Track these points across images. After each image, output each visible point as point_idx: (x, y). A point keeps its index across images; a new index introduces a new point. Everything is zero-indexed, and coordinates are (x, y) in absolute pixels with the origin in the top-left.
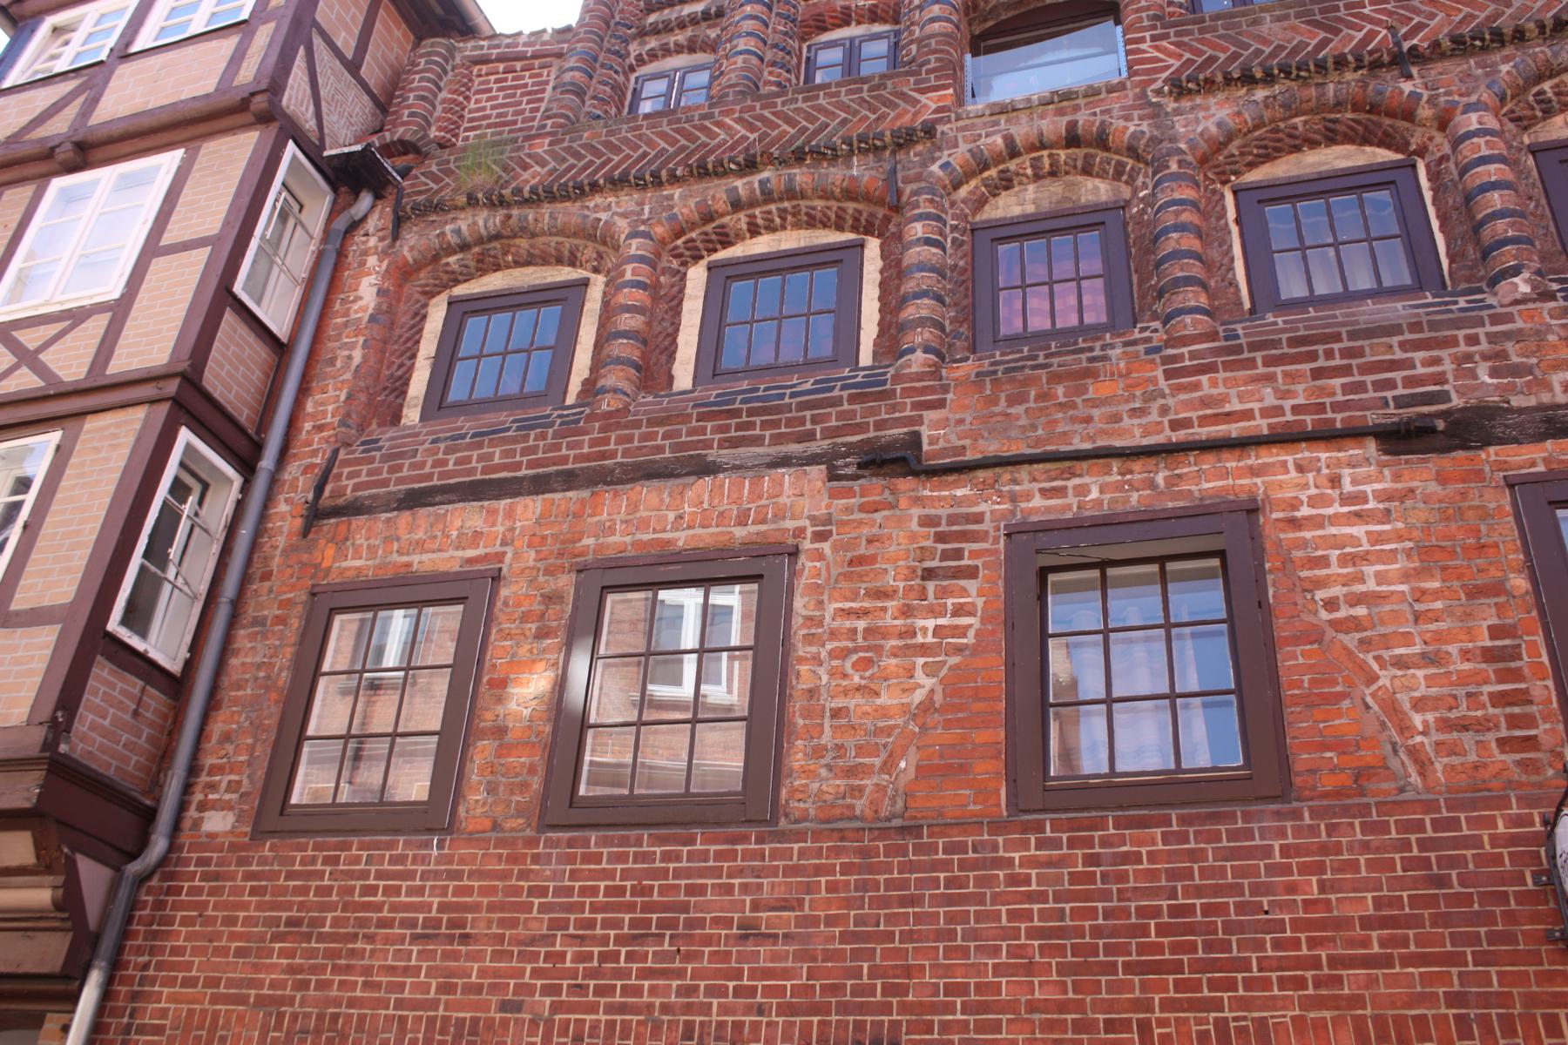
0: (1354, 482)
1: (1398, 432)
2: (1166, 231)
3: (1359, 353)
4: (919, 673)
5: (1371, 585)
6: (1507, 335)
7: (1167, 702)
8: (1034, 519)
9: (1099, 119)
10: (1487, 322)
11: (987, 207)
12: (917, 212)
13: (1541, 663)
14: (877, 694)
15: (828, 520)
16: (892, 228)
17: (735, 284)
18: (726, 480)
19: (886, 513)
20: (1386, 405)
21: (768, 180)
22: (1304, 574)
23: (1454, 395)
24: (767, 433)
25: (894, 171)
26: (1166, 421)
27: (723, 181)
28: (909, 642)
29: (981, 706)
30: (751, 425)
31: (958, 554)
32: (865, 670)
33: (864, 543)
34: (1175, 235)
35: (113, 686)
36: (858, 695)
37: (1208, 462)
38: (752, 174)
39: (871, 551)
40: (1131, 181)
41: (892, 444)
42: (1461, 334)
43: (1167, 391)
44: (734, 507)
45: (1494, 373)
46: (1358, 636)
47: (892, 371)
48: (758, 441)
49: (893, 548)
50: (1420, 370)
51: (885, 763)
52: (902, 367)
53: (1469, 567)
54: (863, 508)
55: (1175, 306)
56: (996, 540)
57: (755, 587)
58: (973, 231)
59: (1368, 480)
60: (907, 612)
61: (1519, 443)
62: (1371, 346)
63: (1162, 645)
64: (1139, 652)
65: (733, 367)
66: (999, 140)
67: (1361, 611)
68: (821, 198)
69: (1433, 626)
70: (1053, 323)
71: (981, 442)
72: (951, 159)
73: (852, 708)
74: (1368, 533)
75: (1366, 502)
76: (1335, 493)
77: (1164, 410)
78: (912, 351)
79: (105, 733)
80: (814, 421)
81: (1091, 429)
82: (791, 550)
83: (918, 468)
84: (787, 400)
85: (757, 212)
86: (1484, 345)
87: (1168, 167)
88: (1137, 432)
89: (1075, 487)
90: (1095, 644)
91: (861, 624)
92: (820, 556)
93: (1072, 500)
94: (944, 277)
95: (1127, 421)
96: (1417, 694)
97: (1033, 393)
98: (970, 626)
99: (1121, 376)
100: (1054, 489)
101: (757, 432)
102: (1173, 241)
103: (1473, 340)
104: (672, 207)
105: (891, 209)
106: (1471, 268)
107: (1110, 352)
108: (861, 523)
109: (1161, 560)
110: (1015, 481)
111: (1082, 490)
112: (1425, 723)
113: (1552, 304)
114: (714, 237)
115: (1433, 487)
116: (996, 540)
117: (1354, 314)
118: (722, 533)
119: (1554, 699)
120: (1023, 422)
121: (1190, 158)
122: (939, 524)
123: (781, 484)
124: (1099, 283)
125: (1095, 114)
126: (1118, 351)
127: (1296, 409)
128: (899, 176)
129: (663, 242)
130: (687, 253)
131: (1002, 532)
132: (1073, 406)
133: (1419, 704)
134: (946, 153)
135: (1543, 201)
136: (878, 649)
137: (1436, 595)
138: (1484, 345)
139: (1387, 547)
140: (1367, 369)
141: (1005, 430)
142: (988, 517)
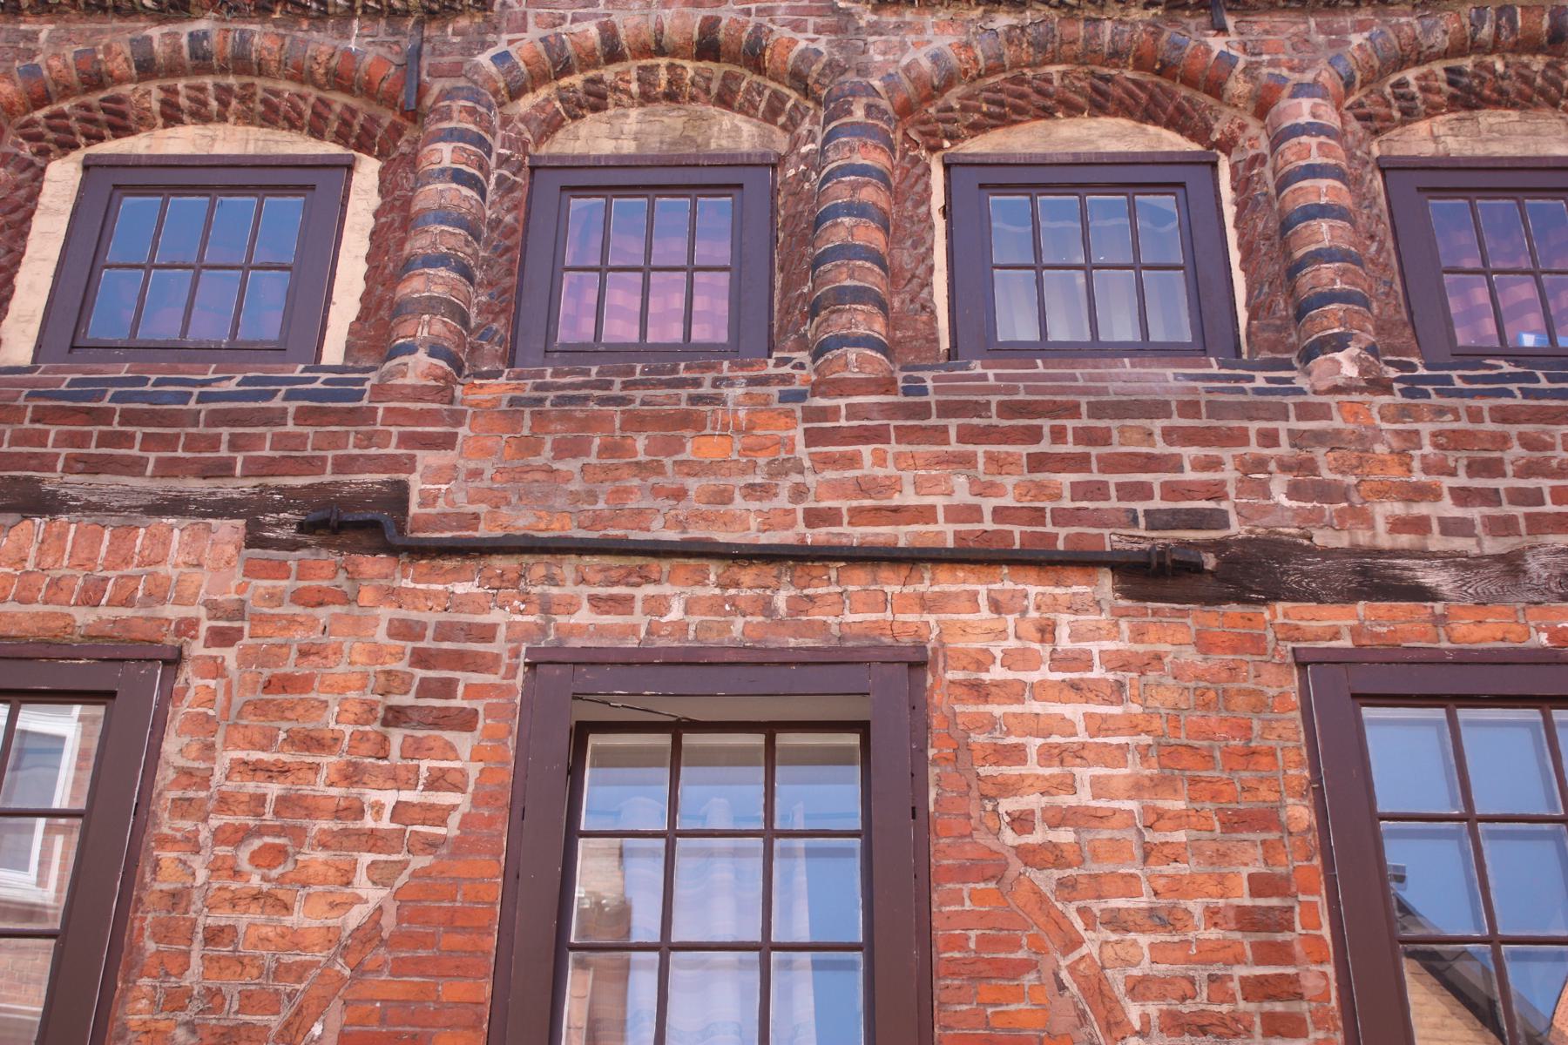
0: (1075, 636)
1: (1147, 565)
2: (835, 212)
3: (1103, 438)
4: (361, 878)
5: (1084, 798)
6: (1319, 438)
7: (755, 955)
8: (576, 643)
9: (753, 20)
10: (1292, 414)
11: (560, 134)
12: (446, 125)
13: (1320, 938)
14: (287, 908)
15: (239, 612)
16: (403, 146)
17: (128, 200)
18: (70, 527)
19: (337, 609)
20: (1135, 521)
21: (205, 35)
22: (986, 770)
23: (1233, 519)
24: (152, 456)
25: (417, 53)
26: (799, 510)
27: (128, 24)
28: (351, 825)
29: (458, 939)
30: (127, 440)
31: (447, 689)
32: (270, 867)
33: (294, 654)
34: (846, 220)
36: (254, 907)
37: (857, 581)
38: (180, 20)
39: (305, 669)
40: (791, 126)
41: (360, 498)
42: (1254, 427)
43: (807, 463)
44: (80, 573)
45: (1294, 491)
46: (1057, 874)
47: (373, 378)
48: (134, 467)
49: (342, 668)
50: (1189, 475)
51: (288, 1025)
52: (392, 374)
53: (1230, 782)
54: (298, 598)
55: (835, 331)
56: (511, 672)
57: (99, 711)
58: (533, 169)
59: (1095, 633)
60: (352, 775)
61: (1320, 602)
62: (1122, 430)
63: (758, 863)
64: (722, 871)
65: (106, 337)
66: (592, 30)
67: (1065, 836)
68: (291, 78)
69: (1170, 869)
70: (643, 333)
71: (504, 510)
72: (512, 49)
73: (242, 929)
74: (1088, 716)
75: (1090, 668)
76: (1045, 650)
77: (799, 493)
78: (410, 350)
80: (234, 444)
81: (682, 509)
82: (168, 655)
83: (398, 541)
84: (192, 405)
85: (181, 84)
86: (1284, 449)
87: (850, 113)
88: (754, 522)
89: (647, 599)
90: (652, 853)
91: (274, 790)
92: (218, 670)
93: (640, 619)
94: (477, 238)
95: (739, 503)
96: (1136, 972)
97: (597, 441)
98: (454, 807)
99: (738, 430)
100: (612, 598)
101: (136, 451)
102: (844, 230)
103: (1270, 438)
104: (32, 54)
105: (404, 114)
106: (1278, 329)
107: (725, 391)
108: (292, 621)
109: (770, 729)
110: (551, 580)
111: (657, 606)
112: (1145, 1019)
113: (1385, 399)
114: (101, 116)
115: (1190, 655)
116: (511, 672)
117: (1102, 378)
118: (54, 616)
119: (1334, 994)
120: (575, 486)
121: (884, 103)
122: (421, 637)
123: (166, 544)
124: (723, 279)
125: (748, 12)
126: (739, 391)
127: (1000, 514)
128: (425, 63)
130: (51, 135)
131: (522, 659)
132: (658, 469)
133: (1138, 988)
134: (505, 37)
135: (1390, 244)
136: (298, 834)
137: (1179, 821)
138: (1284, 449)
139: (1114, 740)
140: (1108, 464)
141: (546, 496)
142: (502, 632)
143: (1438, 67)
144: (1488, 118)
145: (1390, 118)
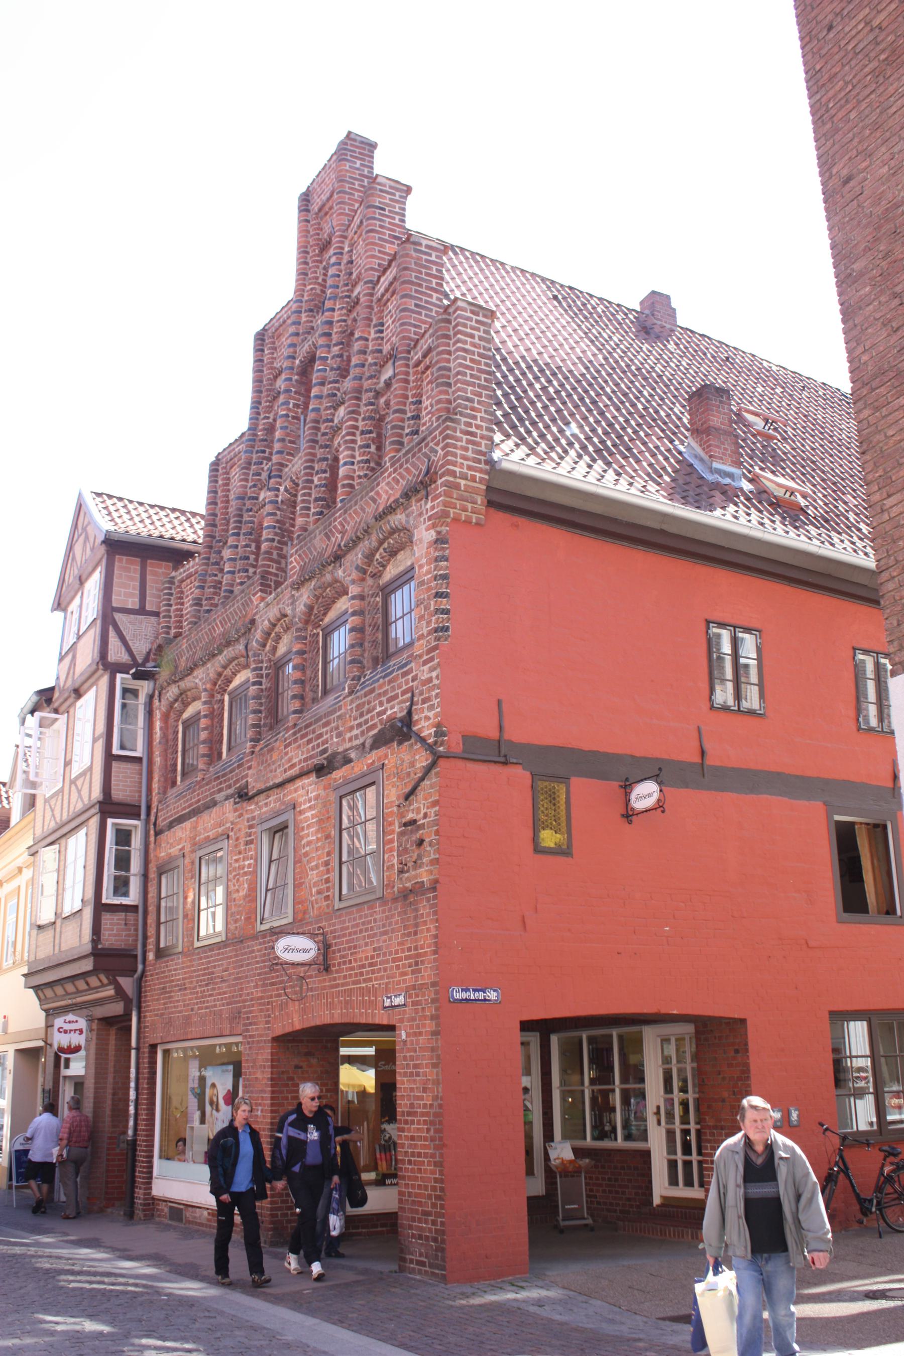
35: (113, 919)
79: (115, 935)
129: (212, 690)
143: (381, 550)
144: (400, 556)
145: (380, 571)
